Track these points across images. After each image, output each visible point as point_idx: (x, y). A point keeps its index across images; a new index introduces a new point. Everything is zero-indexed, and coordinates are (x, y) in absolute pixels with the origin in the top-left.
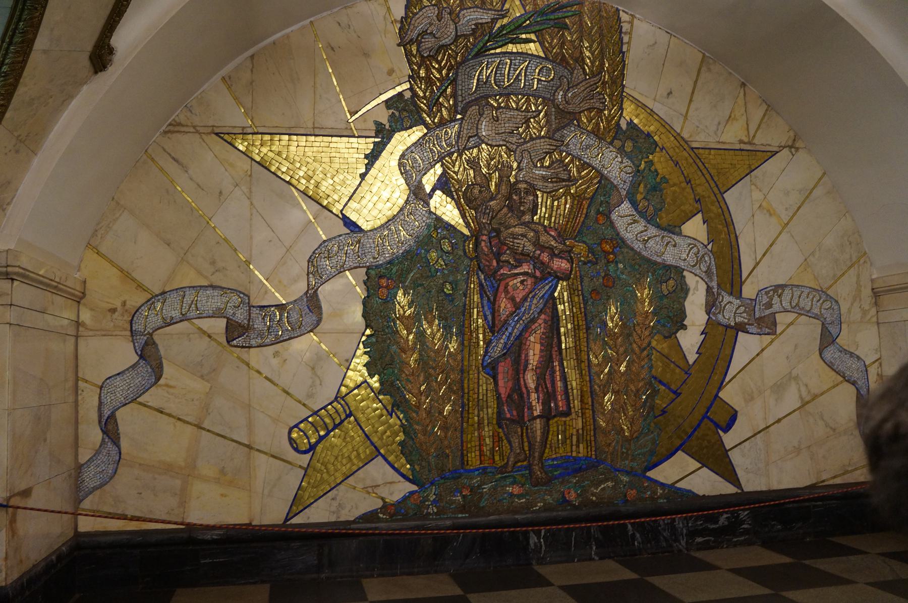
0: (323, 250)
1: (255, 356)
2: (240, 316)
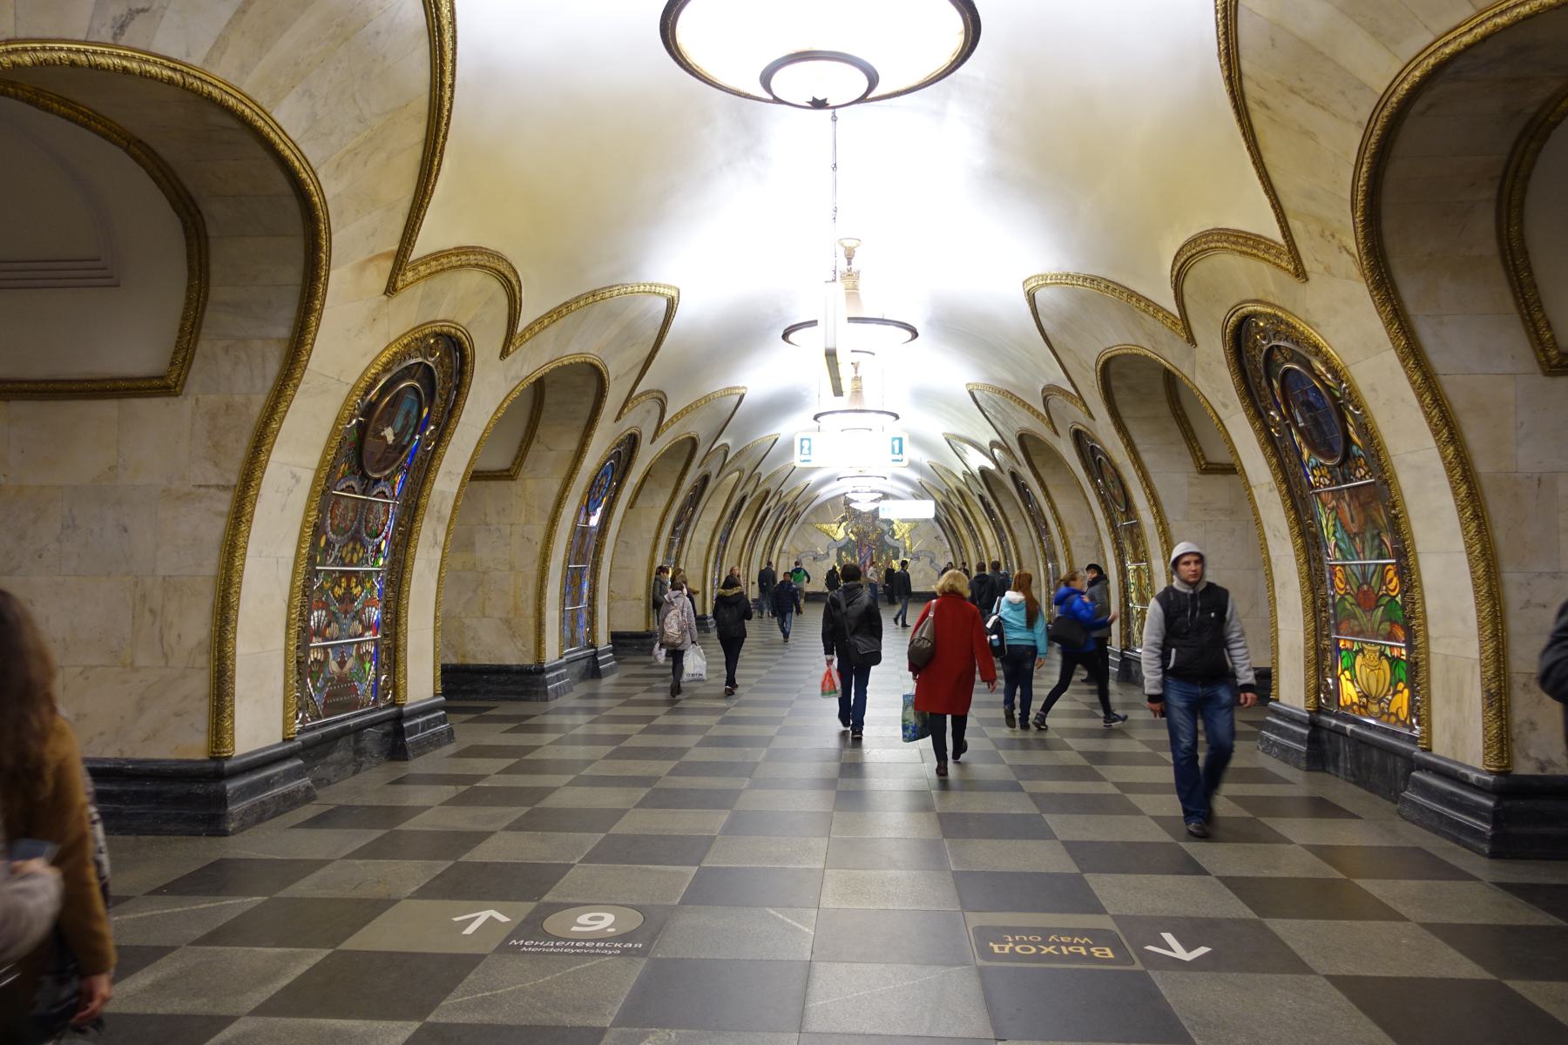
0: (830, 545)
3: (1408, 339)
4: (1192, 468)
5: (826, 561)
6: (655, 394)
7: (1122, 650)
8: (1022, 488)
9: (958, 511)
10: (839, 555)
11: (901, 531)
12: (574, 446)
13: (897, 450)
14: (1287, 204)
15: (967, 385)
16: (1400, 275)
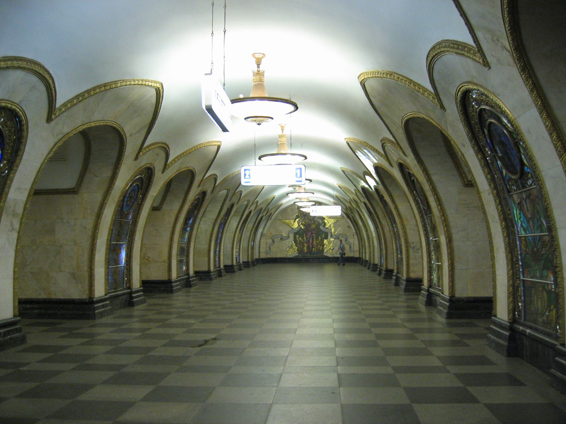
0: (289, 231)
1: (284, 241)
2: (281, 237)
3: (542, 101)
4: (460, 183)
5: (287, 240)
6: (160, 145)
7: (428, 288)
8: (381, 197)
9: (356, 211)
10: (295, 237)
11: (329, 223)
12: (109, 174)
13: (299, 175)
14: (473, 22)
15: (345, 139)
16: (535, 63)
